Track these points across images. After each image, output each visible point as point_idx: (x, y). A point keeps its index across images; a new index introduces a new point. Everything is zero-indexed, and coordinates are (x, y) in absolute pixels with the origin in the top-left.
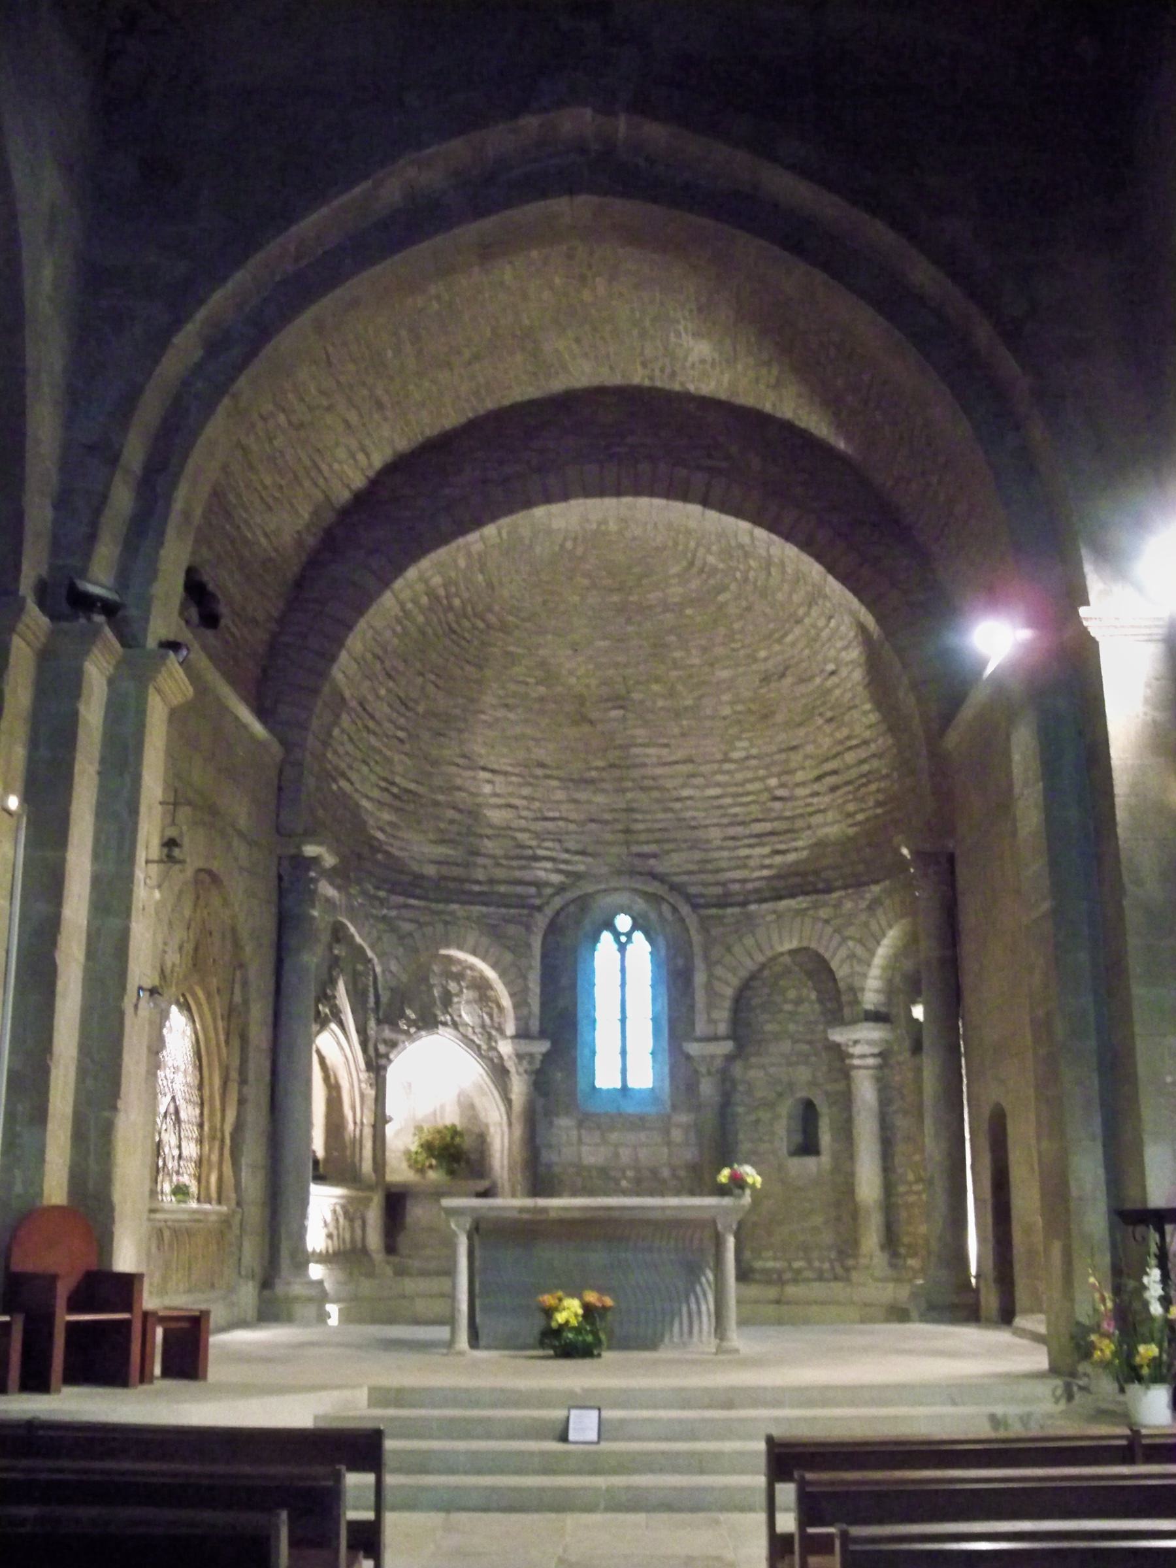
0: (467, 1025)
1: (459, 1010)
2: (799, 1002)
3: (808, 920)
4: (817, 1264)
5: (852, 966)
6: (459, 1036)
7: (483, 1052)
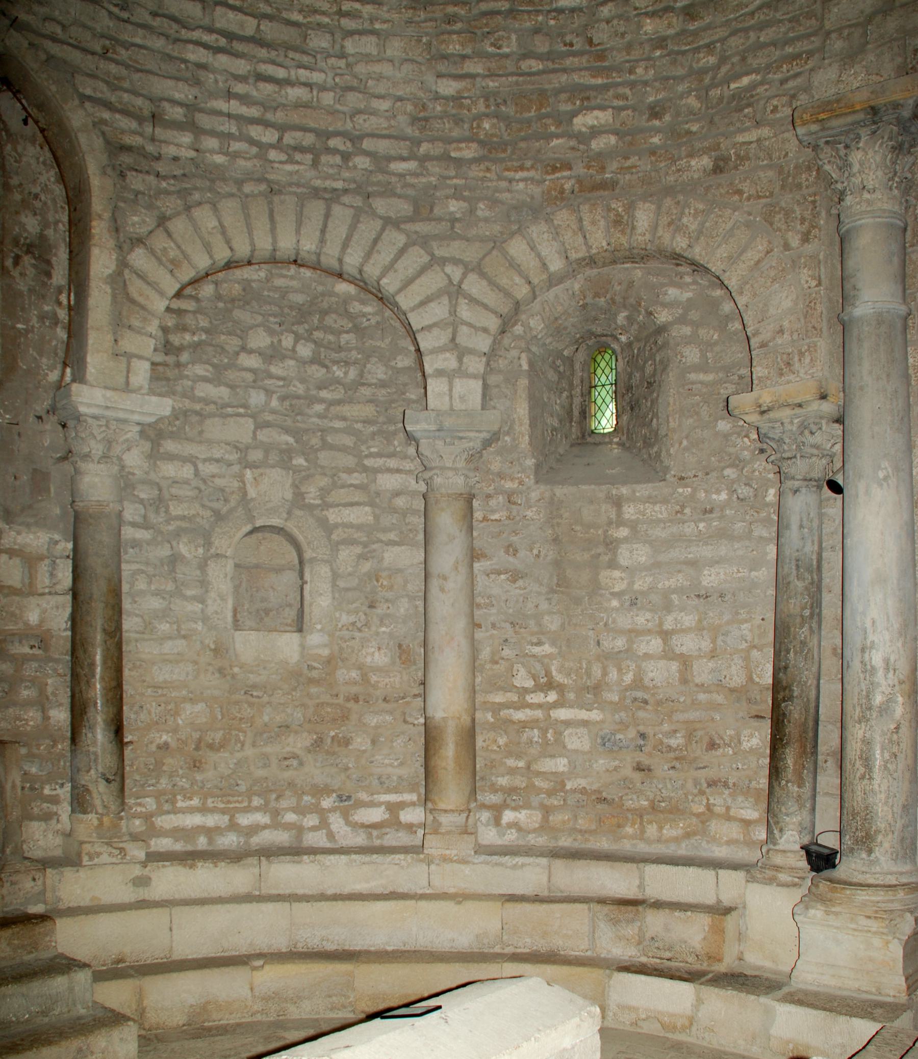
2: (273, 355)
3: (341, 214)
4: (290, 817)
5: (453, 312)
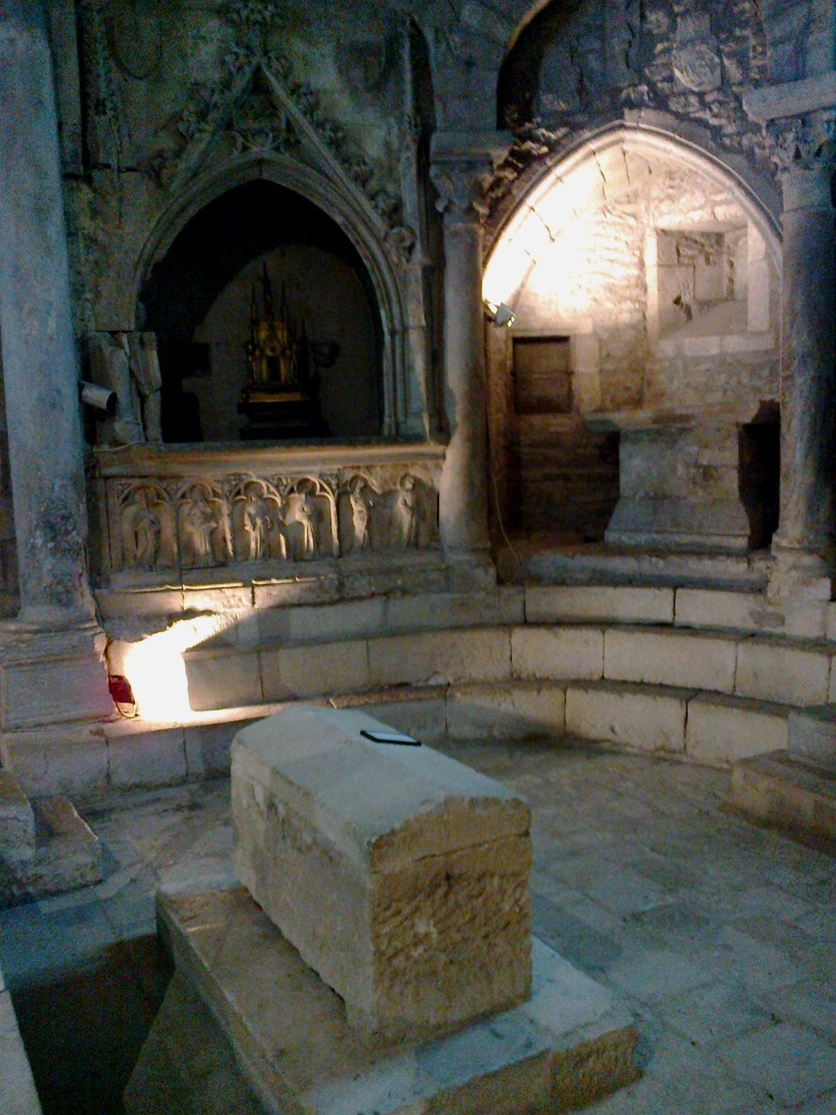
0: (685, 93)
1: (668, 65)
6: (670, 120)
7: (727, 141)
